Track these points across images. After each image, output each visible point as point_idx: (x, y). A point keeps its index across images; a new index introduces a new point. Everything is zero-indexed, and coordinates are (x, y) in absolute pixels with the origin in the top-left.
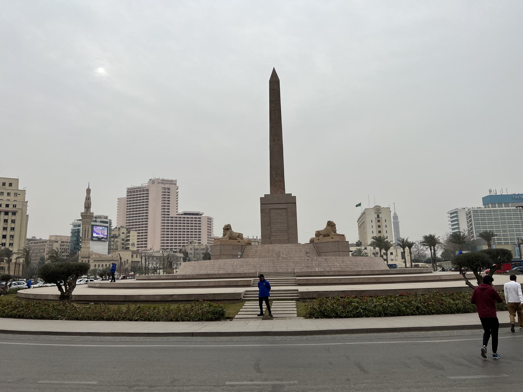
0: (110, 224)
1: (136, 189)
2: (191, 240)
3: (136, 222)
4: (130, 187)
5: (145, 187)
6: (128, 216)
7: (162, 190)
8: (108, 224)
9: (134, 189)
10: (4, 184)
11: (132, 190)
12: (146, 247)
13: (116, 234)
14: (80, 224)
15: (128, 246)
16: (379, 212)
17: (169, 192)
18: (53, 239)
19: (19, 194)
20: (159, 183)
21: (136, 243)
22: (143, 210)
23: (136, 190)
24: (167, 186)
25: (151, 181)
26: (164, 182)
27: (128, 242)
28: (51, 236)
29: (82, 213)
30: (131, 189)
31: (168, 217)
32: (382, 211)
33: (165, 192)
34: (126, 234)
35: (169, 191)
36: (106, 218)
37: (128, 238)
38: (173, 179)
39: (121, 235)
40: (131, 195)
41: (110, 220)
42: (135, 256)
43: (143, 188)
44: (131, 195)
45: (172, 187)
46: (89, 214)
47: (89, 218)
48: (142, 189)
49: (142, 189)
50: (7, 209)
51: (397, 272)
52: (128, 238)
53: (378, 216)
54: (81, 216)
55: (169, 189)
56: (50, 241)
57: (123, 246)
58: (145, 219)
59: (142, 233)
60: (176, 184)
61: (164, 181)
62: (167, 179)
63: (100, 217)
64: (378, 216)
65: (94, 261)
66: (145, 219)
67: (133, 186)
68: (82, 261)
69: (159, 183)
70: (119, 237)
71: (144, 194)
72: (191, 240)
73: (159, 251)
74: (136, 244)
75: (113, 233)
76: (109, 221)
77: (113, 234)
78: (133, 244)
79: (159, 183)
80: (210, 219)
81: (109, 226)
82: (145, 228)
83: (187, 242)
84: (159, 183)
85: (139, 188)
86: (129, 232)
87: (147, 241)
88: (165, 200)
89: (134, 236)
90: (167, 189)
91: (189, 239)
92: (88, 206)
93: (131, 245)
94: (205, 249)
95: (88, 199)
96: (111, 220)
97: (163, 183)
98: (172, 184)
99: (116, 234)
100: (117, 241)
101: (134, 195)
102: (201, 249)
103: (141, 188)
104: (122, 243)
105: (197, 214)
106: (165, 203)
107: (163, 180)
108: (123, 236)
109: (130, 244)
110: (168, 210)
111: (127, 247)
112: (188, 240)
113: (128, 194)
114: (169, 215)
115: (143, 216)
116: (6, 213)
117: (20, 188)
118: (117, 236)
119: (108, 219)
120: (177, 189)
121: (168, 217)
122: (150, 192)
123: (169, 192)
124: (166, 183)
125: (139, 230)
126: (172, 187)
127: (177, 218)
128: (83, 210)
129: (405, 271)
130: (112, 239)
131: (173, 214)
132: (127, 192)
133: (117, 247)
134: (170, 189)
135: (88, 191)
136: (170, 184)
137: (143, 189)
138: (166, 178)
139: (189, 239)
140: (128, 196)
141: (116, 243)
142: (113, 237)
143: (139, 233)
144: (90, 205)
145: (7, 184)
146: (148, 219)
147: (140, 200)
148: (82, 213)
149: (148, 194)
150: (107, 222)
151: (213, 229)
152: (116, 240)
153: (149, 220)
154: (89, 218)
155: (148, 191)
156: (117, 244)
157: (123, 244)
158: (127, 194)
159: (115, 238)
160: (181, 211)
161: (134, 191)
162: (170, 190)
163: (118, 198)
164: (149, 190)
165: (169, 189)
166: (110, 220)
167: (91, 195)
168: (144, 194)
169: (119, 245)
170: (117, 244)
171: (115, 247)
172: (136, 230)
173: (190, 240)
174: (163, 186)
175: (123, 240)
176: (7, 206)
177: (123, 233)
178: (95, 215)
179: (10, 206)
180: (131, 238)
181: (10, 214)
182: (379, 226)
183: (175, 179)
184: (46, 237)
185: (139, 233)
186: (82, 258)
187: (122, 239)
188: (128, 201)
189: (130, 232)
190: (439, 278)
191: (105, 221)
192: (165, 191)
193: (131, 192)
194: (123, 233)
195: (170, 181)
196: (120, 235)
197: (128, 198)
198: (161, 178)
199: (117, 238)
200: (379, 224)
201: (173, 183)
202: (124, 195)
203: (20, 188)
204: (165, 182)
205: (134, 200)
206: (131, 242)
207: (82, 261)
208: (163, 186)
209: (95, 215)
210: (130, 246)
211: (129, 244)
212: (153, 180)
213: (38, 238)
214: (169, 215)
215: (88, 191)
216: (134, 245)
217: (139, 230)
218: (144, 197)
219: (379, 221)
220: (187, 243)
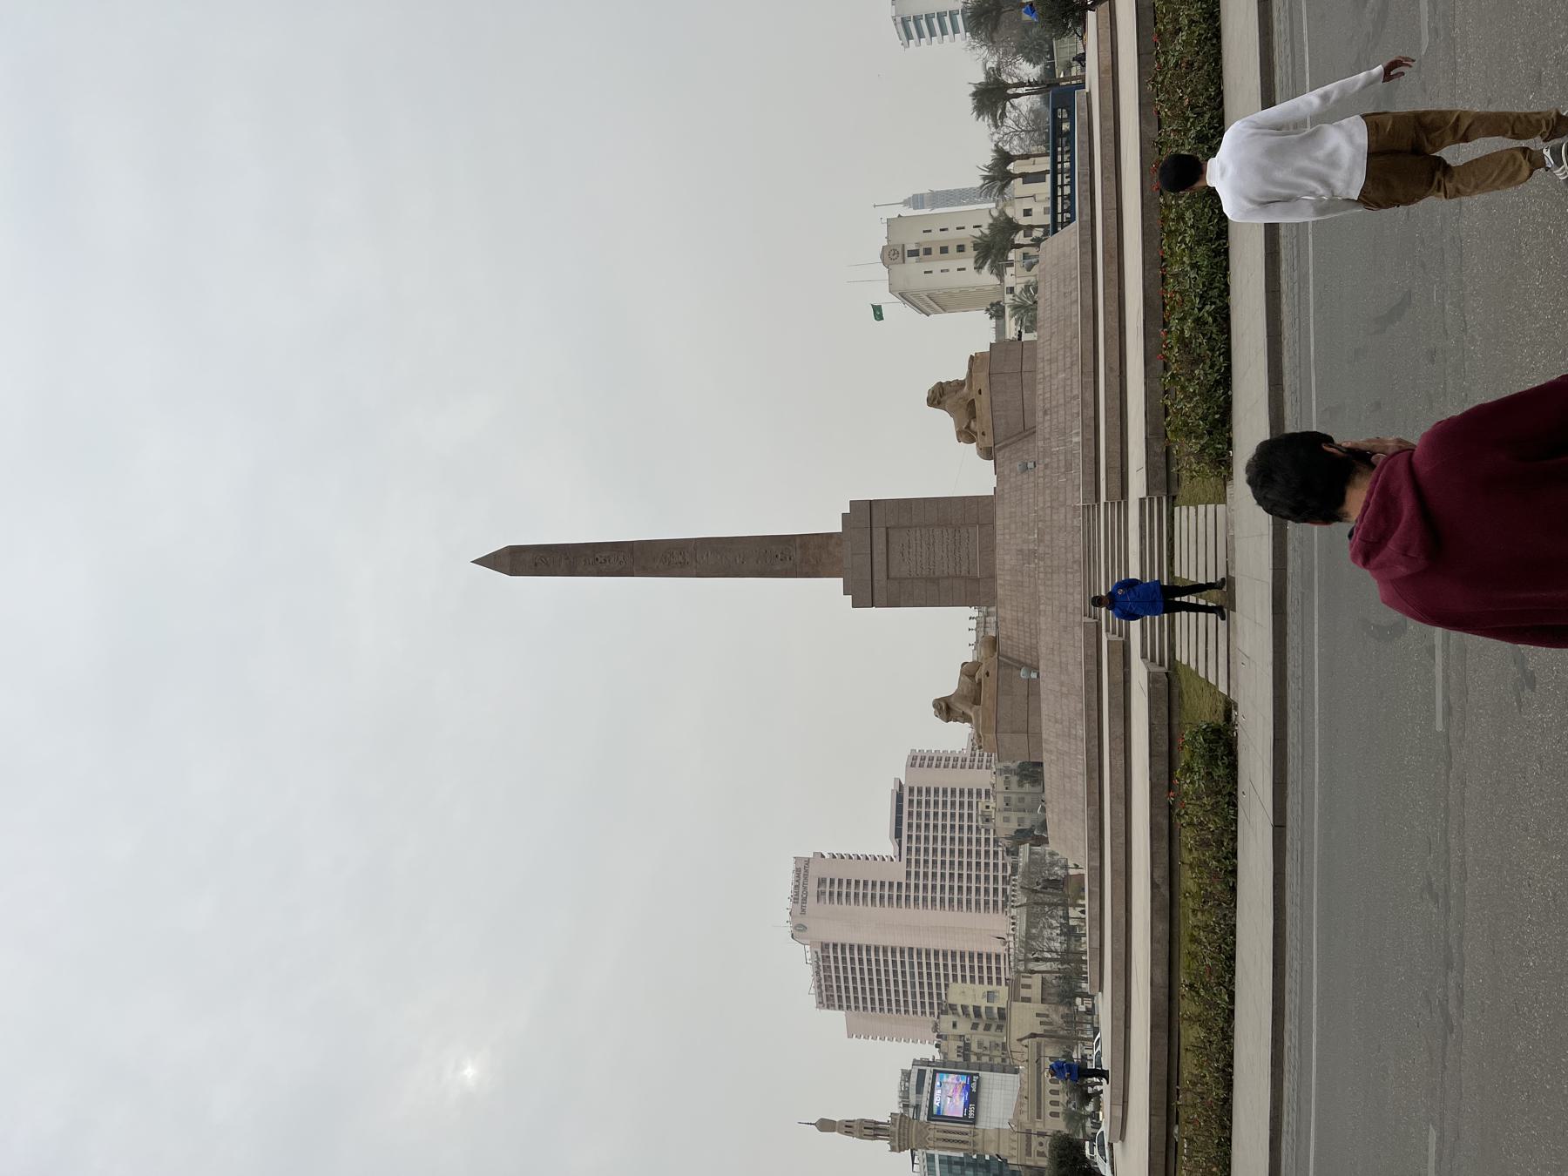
0: (928, 1063)
1: (819, 981)
2: (980, 819)
3: (921, 984)
4: (813, 999)
5: (816, 952)
6: (902, 1009)
7: (825, 903)
9: (819, 987)
12: (998, 956)
13: (959, 1047)
14: (925, 1155)
15: (996, 1011)
16: (900, 250)
17: (832, 881)
21: (986, 987)
24: (813, 887)
26: (799, 897)
27: (983, 1010)
29: (893, 1149)
30: (820, 994)
31: (908, 886)
33: (831, 894)
34: (959, 1016)
35: (828, 881)
36: (906, 1075)
37: (971, 1010)
38: (792, 867)
40: (840, 997)
41: (915, 1063)
42: (1024, 993)
43: (818, 959)
44: (840, 997)
45: (815, 872)
46: (895, 1126)
47: (907, 1126)
48: (821, 963)
49: (821, 963)
51: (1086, 199)
52: (971, 1010)
53: (914, 253)
54: (900, 1151)
55: (821, 882)
57: (994, 1027)
58: (911, 956)
60: (808, 861)
63: (905, 1094)
64: (914, 253)
66: (911, 956)
67: (813, 991)
69: (803, 911)
70: (968, 1040)
71: (836, 958)
72: (980, 819)
73: (1012, 918)
74: (990, 988)
75: (953, 1056)
78: (990, 996)
80: (915, 758)
81: (932, 1069)
83: (983, 830)
84: (803, 911)
85: (818, 973)
86: (953, 1007)
87: (978, 954)
90: (822, 889)
91: (974, 824)
92: (871, 1130)
94: (1007, 778)
95: (848, 1128)
96: (915, 1060)
97: (805, 900)
98: (806, 871)
99: (959, 1047)
100: (980, 1045)
101: (839, 987)
102: (1007, 788)
103: (818, 967)
104: (984, 1030)
105: (899, 798)
106: (865, 896)
107: (795, 900)
108: (964, 1027)
109: (989, 1005)
111: (996, 1016)
112: (977, 827)
113: (837, 1006)
114: (899, 885)
115: (903, 963)
119: (909, 1067)
120: (823, 856)
121: (908, 886)
123: (832, 881)
124: (805, 888)
125: (946, 976)
126: (815, 872)
127: (909, 861)
128: (883, 1145)
130: (973, 1059)
131: (897, 873)
132: (828, 1008)
133: (998, 1045)
134: (821, 876)
135: (825, 1125)
139: (974, 824)
140: (840, 1007)
142: (966, 1058)
143: (955, 977)
144: (866, 1121)
146: (911, 949)
147: (853, 969)
148: (893, 1149)
149: (835, 946)
150: (921, 1074)
152: (974, 1047)
153: (916, 946)
154: (907, 1126)
155: (827, 945)
156: (987, 1044)
157: (987, 1028)
159: (969, 1050)
160: (889, 849)
161: (828, 988)
164: (826, 941)
166: (913, 1065)
168: (836, 958)
169: (992, 1038)
170: (987, 1044)
171: (996, 1053)
172: (947, 986)
173: (977, 821)
174: (812, 899)
175: (975, 1026)
177: (955, 1025)
178: (898, 1110)
180: (970, 1003)
182: (944, 250)
183: (793, 861)
185: (955, 977)
186: (1029, 1153)
187: (972, 1029)
189: (950, 1005)
190: (1106, 71)
192: (827, 893)
194: (955, 1025)
196: (961, 1036)
198: (789, 904)
199: (969, 1045)
200: (936, 251)
201: (803, 869)
202: (838, 1017)
204: (800, 893)
206: (983, 1004)
207: (1041, 1154)
208: (812, 899)
209: (898, 1110)
210: (995, 1006)
212: (795, 928)
214: (899, 885)
215: (825, 1125)
217: (946, 976)
218: (844, 959)
219: (928, 251)
220: (987, 831)
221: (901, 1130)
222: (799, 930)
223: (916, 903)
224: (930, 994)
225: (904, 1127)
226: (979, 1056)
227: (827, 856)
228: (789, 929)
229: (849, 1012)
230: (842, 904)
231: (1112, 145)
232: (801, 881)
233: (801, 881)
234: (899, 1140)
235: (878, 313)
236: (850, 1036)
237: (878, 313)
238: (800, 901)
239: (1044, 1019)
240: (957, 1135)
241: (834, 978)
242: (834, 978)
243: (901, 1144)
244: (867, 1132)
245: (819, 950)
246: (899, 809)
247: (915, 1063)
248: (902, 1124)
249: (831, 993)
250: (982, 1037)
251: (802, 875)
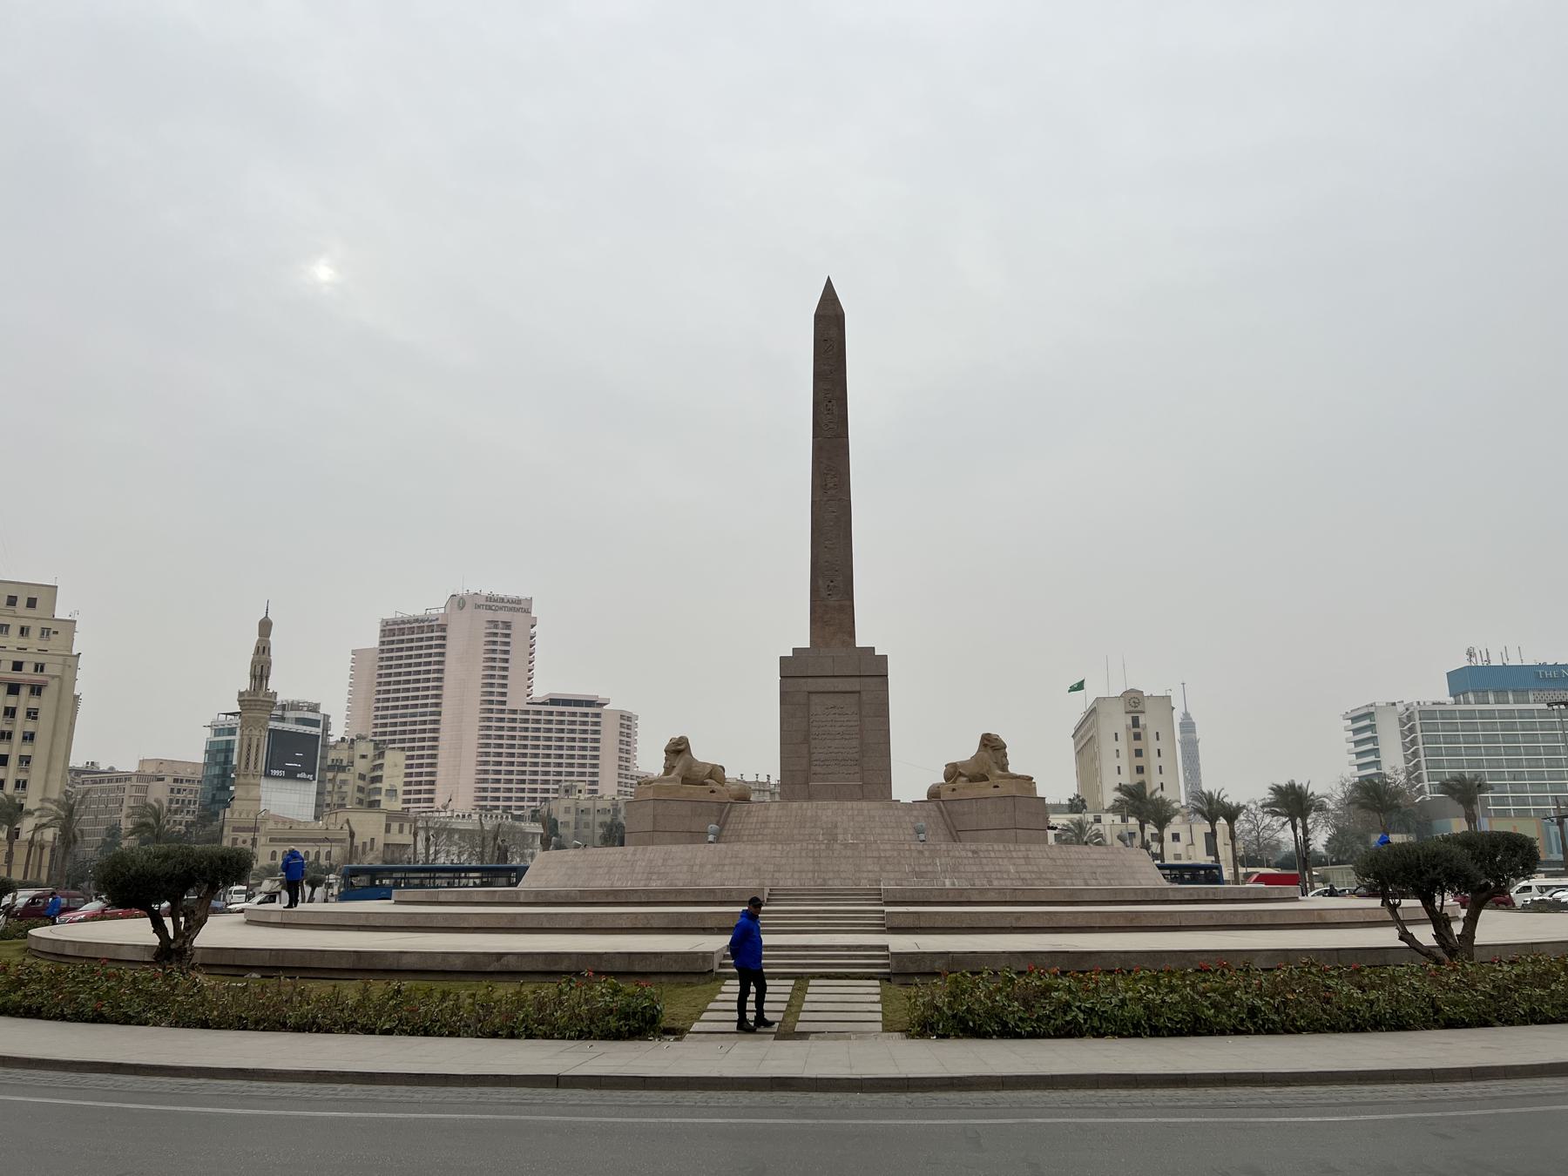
0: (326, 729)
1: (409, 622)
2: (568, 783)
3: (405, 724)
4: (390, 616)
5: (437, 619)
6: (380, 705)
7: (486, 628)
8: (318, 727)
9: (403, 622)
10: (12, 601)
11: (396, 627)
12: (431, 800)
13: (342, 760)
14: (234, 726)
15: (377, 798)
16: (1139, 708)
17: (507, 636)
18: (150, 770)
19: (57, 633)
20: (479, 607)
21: (401, 788)
23: (409, 626)
24: (503, 616)
25: (456, 599)
26: (493, 602)
27: (378, 785)
28: (142, 762)
29: (241, 694)
30: (395, 623)
31: (502, 711)
32: (1148, 706)
33: (495, 634)
34: (373, 761)
36: (314, 708)
37: (379, 773)
38: (522, 596)
40: (392, 642)
41: (327, 717)
42: (395, 826)
44: (392, 642)
45: (517, 619)
47: (264, 708)
48: (426, 624)
49: (426, 624)
51: (1191, 894)
52: (379, 773)
53: (1135, 722)
54: (239, 701)
55: (507, 625)
56: (140, 776)
57: (361, 796)
58: (432, 714)
59: (422, 757)
60: (528, 611)
61: (495, 601)
63: (295, 706)
64: (1135, 722)
65: (271, 840)
66: (432, 714)
67: (399, 615)
68: (235, 840)
70: (349, 770)
72: (568, 783)
73: (470, 815)
74: (400, 792)
75: (332, 755)
78: (392, 792)
79: (479, 607)
80: (629, 719)
81: (320, 734)
83: (557, 787)
85: (417, 621)
86: (381, 755)
90: (501, 625)
91: (563, 778)
92: (260, 672)
93: (386, 795)
94: (609, 811)
95: (263, 650)
96: (329, 717)
97: (490, 608)
98: (518, 610)
99: (342, 760)
100: (344, 782)
101: (402, 641)
102: (598, 811)
103: (423, 621)
104: (359, 786)
105: (590, 703)
106: (493, 668)
107: (490, 598)
108: (362, 766)
109: (383, 792)
110: (503, 690)
111: (372, 798)
112: (560, 781)
114: (504, 703)
115: (426, 705)
116: (13, 689)
117: (60, 613)
119: (322, 710)
120: (533, 626)
121: (502, 711)
122: (450, 634)
123: (507, 636)
124: (501, 609)
125: (412, 749)
127: (527, 712)
128: (245, 684)
129: (1214, 894)
130: (330, 775)
131: (516, 701)
132: (382, 631)
133: (344, 799)
135: (265, 627)
136: (511, 609)
138: (501, 591)
139: (563, 778)
140: (382, 643)
141: (341, 787)
142: (330, 768)
143: (411, 757)
144: (269, 668)
145: (22, 601)
146: (439, 714)
148: (241, 694)
150: (315, 723)
151: (636, 748)
152: (341, 776)
154: (264, 708)
155: (444, 630)
156: (345, 788)
157: (361, 789)
158: (381, 637)
159: (339, 771)
160: (540, 691)
166: (325, 715)
169: (350, 794)
170: (345, 788)
171: (336, 797)
172: (403, 749)
173: (566, 781)
174: (490, 615)
175: (362, 777)
177: (363, 757)
178: (280, 699)
180: (385, 772)
181: (24, 691)
182: (1139, 753)
183: (528, 597)
184: (127, 764)
185: (411, 757)
186: (235, 829)
187: (360, 774)
189: (383, 753)
190: (1320, 916)
194: (363, 757)
196: (352, 762)
197: (382, 651)
198: (485, 592)
199: (344, 771)
200: (1138, 745)
201: (521, 606)
202: (372, 640)
203: (60, 613)
205: (401, 658)
206: (385, 785)
207: (235, 840)
209: (280, 699)
210: (382, 797)
211: (379, 791)
213: (103, 767)
214: (504, 703)
215: (265, 627)
217: (412, 749)
219: (1137, 737)
220: (556, 791)
221: (260, 703)
222: (459, 602)
224: (394, 733)
226: (332, 781)
227: (533, 630)
228: (461, 592)
229: (378, 651)
231: (1245, 922)
232: (507, 605)
233: (507, 605)
235: (1080, 686)
236: (354, 653)
237: (1080, 686)
238: (488, 603)
239: (368, 847)
240: (254, 758)
241: (412, 636)
242: (412, 636)
243: (246, 703)
244: (259, 669)
245: (439, 622)
246: (578, 703)
247: (327, 717)
248: (266, 704)
249: (394, 632)
250: (352, 782)
251: (514, 605)
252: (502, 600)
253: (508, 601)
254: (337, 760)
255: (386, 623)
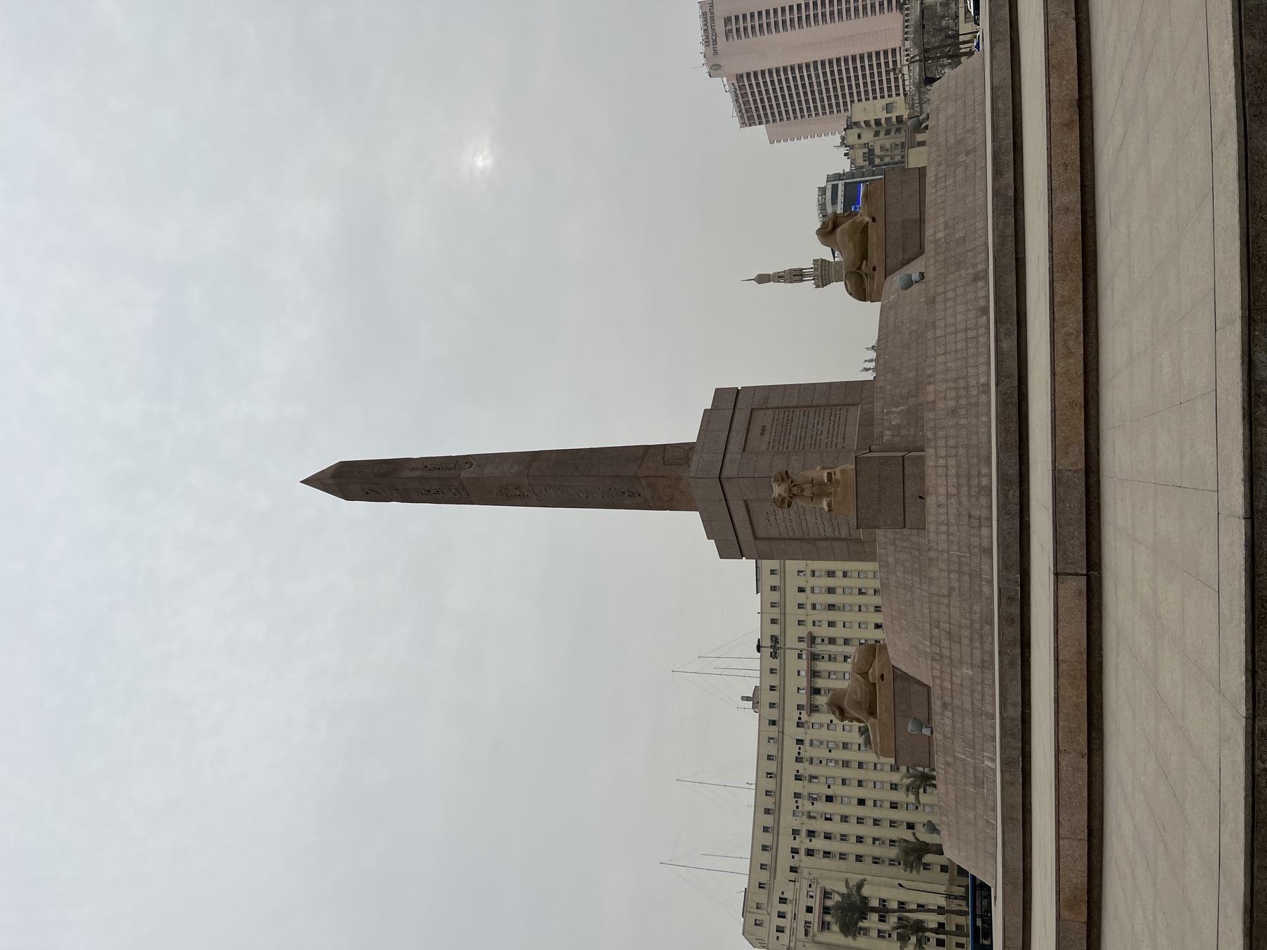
0: (839, 177)
1: (739, 106)
4: (736, 121)
5: (733, 84)
6: (813, 113)
7: (734, 40)
8: (837, 185)
9: (740, 111)
11: (745, 116)
13: (864, 153)
15: (894, 119)
17: (737, 18)
19: (783, 893)
21: (887, 100)
22: (794, 78)
23: (742, 106)
24: (720, 27)
26: (710, 40)
27: (883, 121)
30: (742, 117)
33: (738, 30)
34: (862, 127)
36: (822, 191)
37: (873, 123)
39: (863, 140)
43: (736, 89)
44: (759, 116)
46: (818, 271)
47: (827, 268)
48: (738, 92)
49: (738, 92)
50: (816, 910)
51: (1012, 664)
52: (873, 123)
54: (823, 287)
55: (727, 21)
57: (893, 131)
61: (708, 38)
62: (701, 33)
63: (822, 206)
67: (735, 114)
69: (716, 52)
70: (871, 146)
71: (751, 85)
73: (906, 50)
74: (890, 100)
75: (860, 162)
76: (830, 183)
77: (864, 160)
81: (844, 181)
82: (843, 64)
84: (716, 52)
85: (737, 101)
86: (857, 124)
87: (876, 52)
88: (761, 26)
89: (865, 109)
90: (728, 27)
92: (796, 276)
93: (891, 112)
95: (780, 277)
97: (715, 41)
98: (712, 13)
99: (864, 153)
100: (882, 148)
101: (757, 108)
103: (737, 95)
104: (885, 135)
106: (768, 25)
107: (707, 44)
108: (868, 136)
109: (889, 115)
111: (896, 123)
113: (757, 123)
115: (809, 76)
118: (869, 150)
122: (744, 71)
123: (737, 18)
124: (713, 30)
128: (809, 285)
129: (1011, 599)
130: (877, 161)
132: (750, 126)
133: (897, 145)
134: (726, 17)
135: (762, 279)
136: (713, 21)
137: (738, 89)
138: (698, 35)
140: (760, 123)
141: (887, 150)
142: (871, 162)
144: (795, 270)
146: (815, 62)
147: (767, 91)
148: (818, 286)
149: (748, 75)
150: (835, 188)
152: (877, 152)
153: (818, 59)
154: (827, 268)
155: (741, 76)
156: (888, 146)
157: (888, 132)
159: (873, 155)
161: (746, 103)
162: (731, 18)
163: (771, 144)
164: (740, 72)
165: (727, 21)
166: (827, 182)
167: (771, 271)
168: (751, 85)
169: (892, 141)
170: (888, 146)
171: (898, 152)
174: (721, 39)
175: (877, 134)
176: (809, 910)
177: (859, 137)
179: (810, 905)
180: (871, 118)
183: (698, 6)
187: (874, 136)
188: (774, 121)
189: (854, 122)
190: (1068, 125)
191: (830, 195)
192: (734, 31)
193: (748, 116)
194: (859, 137)
195: (706, 20)
196: (865, 144)
198: (702, 48)
199: (873, 150)
202: (760, 130)
204: (710, 36)
206: (883, 116)
210: (893, 116)
211: (888, 120)
212: (711, 68)
215: (762, 279)
216: (891, 103)
218: (758, 84)
221: (823, 273)
222: (714, 69)
223: (816, 19)
225: (825, 270)
226: (881, 158)
228: (706, 69)
230: (749, 37)
231: (1077, 275)
232: (709, 25)
233: (709, 25)
234: (822, 279)
236: (772, 142)
238: (711, 44)
243: (823, 273)
244: (795, 278)
245: (735, 82)
247: (829, 179)
248: (823, 268)
249: (748, 116)
250: (883, 141)
251: (708, 18)
252: (706, 31)
253: (705, 25)
254: (864, 157)
255: (743, 124)
